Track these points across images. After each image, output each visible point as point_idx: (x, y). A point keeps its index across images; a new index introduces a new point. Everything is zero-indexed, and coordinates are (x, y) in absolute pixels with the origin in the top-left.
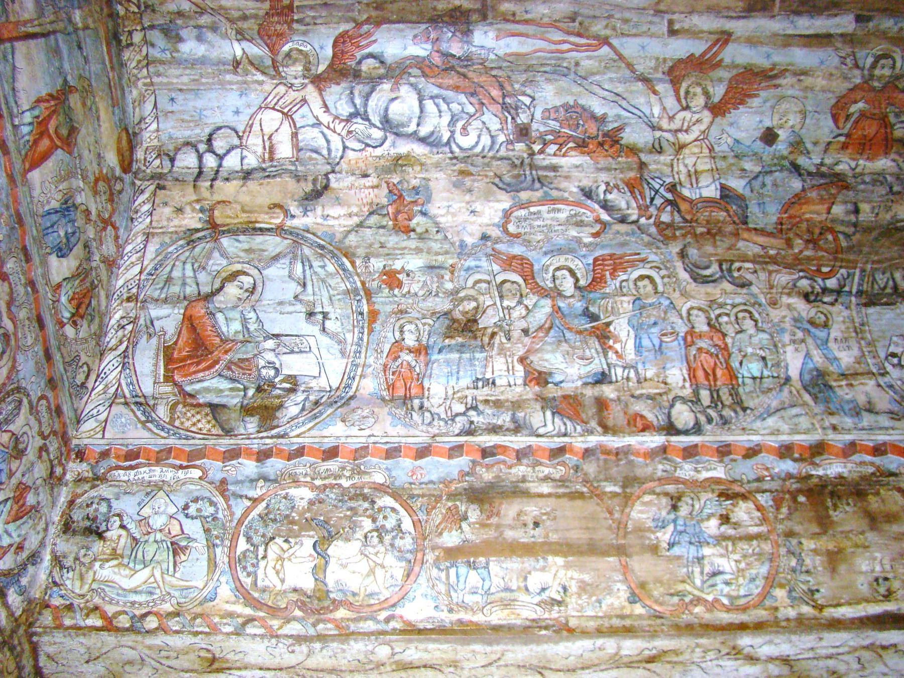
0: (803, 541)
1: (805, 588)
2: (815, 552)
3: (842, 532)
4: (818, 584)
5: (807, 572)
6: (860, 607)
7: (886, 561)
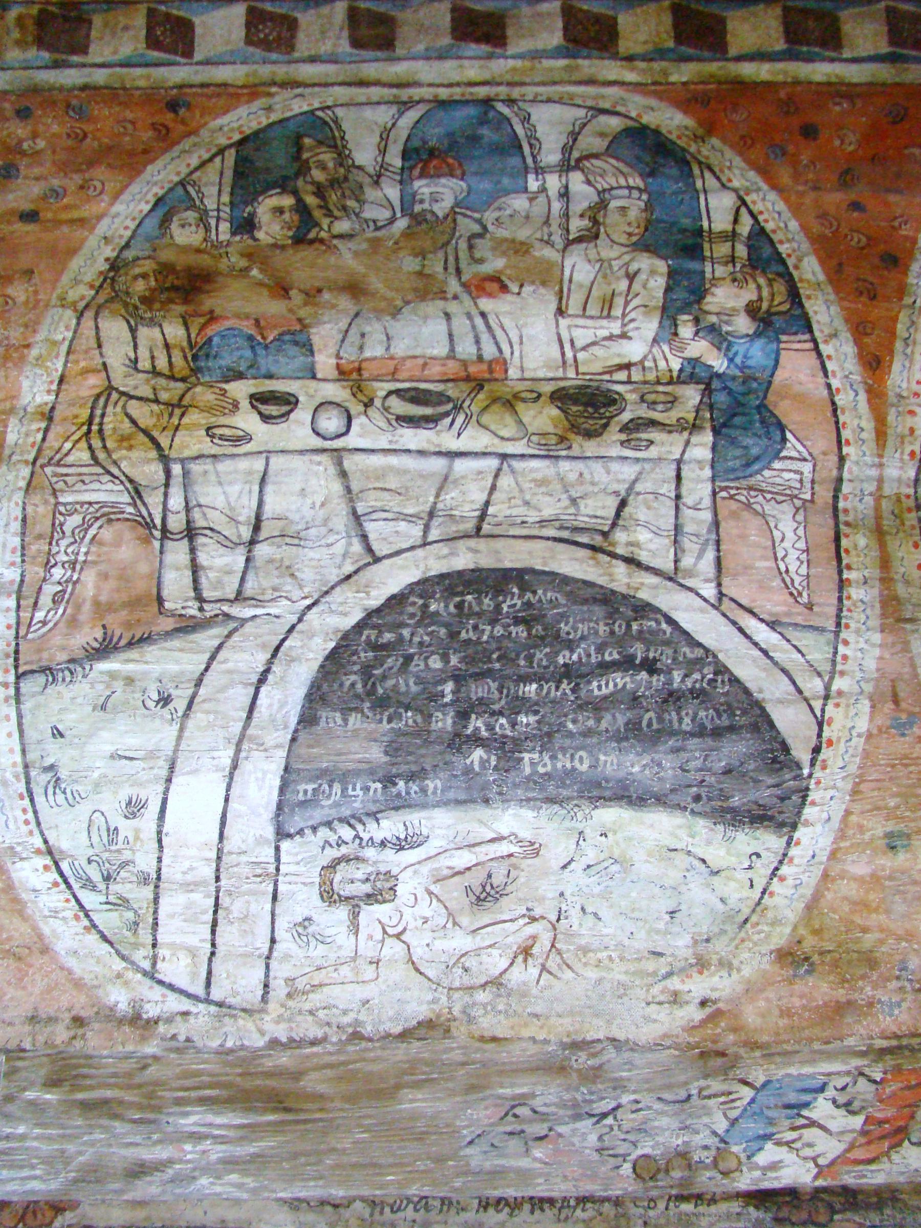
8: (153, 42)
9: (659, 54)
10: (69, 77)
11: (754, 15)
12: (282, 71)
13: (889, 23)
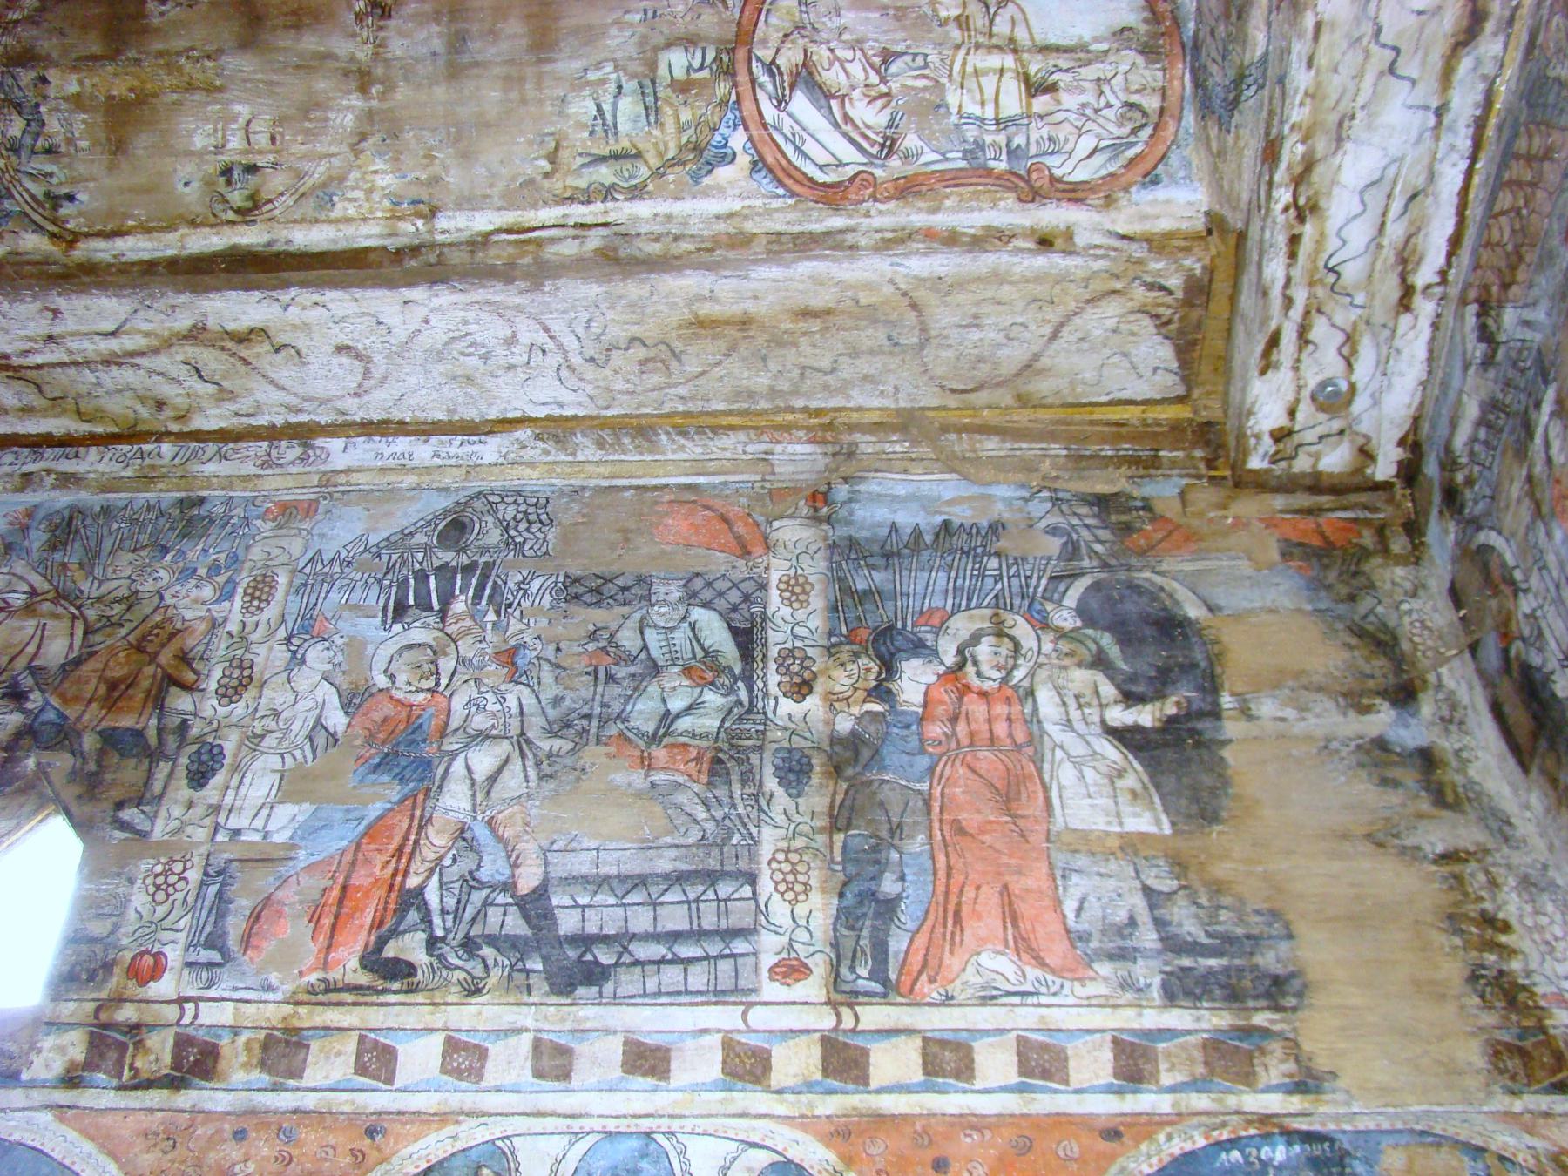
0: (52, 75)
1: (37, 189)
2: (77, 101)
3: (161, 54)
4: (73, 181)
5: (50, 151)
6: (172, 237)
7: (261, 130)
8: (361, 1069)
9: (809, 1087)
10: (284, 1100)
11: (896, 1047)
12: (470, 1100)
13: (1019, 1054)
